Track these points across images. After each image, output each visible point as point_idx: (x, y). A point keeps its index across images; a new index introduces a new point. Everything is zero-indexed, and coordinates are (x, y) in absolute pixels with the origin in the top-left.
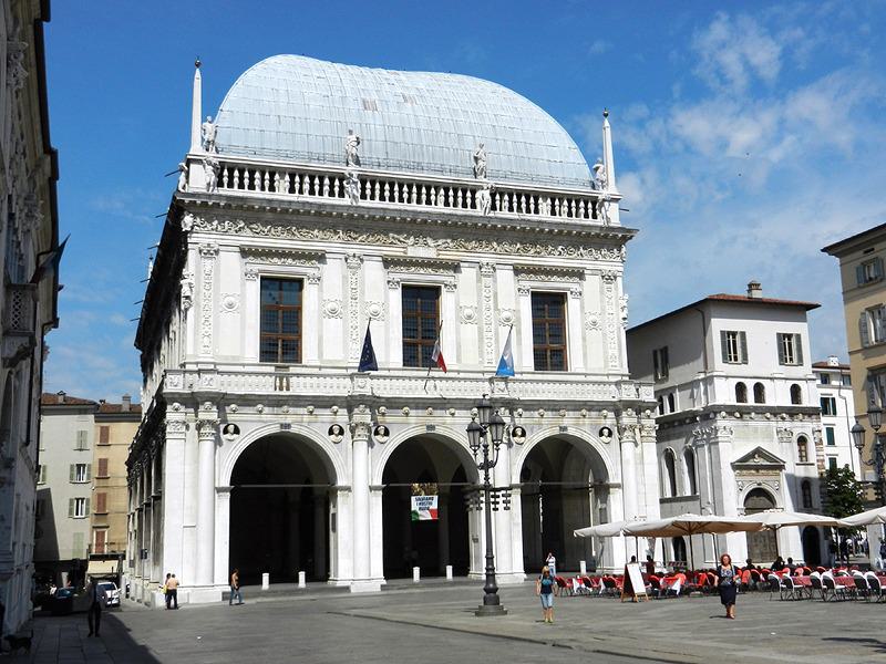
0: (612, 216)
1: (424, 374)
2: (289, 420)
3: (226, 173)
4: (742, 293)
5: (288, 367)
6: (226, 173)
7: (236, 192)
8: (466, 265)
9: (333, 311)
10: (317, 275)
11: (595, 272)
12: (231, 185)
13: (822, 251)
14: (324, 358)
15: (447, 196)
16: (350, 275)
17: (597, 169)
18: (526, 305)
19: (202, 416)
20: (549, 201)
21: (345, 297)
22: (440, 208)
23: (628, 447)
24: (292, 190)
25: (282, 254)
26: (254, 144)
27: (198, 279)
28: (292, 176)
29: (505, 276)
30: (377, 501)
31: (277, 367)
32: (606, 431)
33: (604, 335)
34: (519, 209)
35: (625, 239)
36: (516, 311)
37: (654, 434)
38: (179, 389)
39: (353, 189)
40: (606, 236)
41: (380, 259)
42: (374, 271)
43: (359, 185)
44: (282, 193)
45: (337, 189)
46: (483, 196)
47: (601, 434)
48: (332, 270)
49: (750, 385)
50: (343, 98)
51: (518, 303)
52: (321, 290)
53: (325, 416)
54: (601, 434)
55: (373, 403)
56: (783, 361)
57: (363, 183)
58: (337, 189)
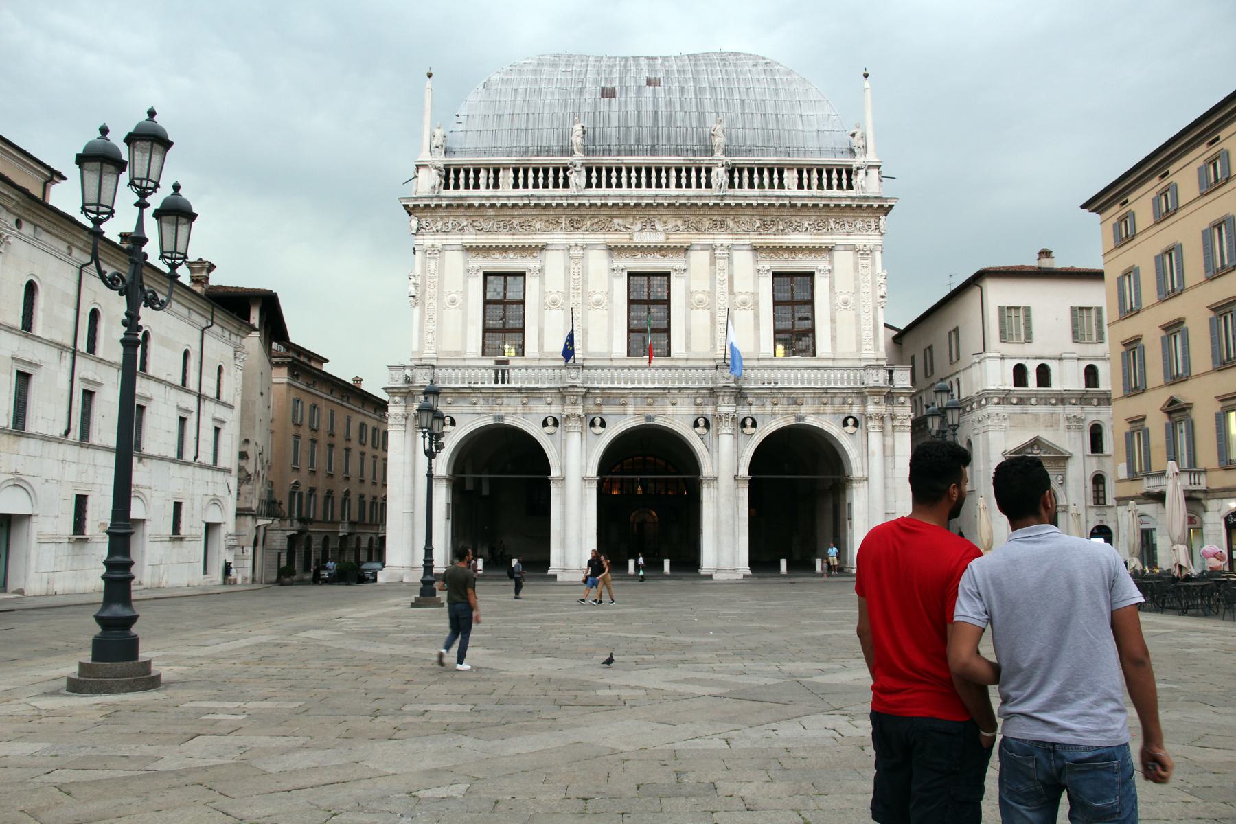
0: (868, 185)
2: (503, 412)
3: (452, 175)
4: (1031, 261)
6: (452, 175)
8: (699, 247)
9: (554, 302)
10: (539, 267)
11: (847, 248)
12: (457, 186)
13: (1084, 206)
14: (546, 349)
15: (679, 178)
16: (573, 265)
17: (853, 135)
18: (767, 284)
20: (795, 174)
21: (567, 288)
23: (875, 439)
24: (516, 186)
25: (504, 249)
26: (486, 143)
27: (424, 278)
28: (516, 171)
29: (743, 259)
31: (498, 362)
32: (850, 421)
33: (858, 316)
34: (761, 186)
35: (886, 210)
36: (755, 294)
37: (909, 424)
39: (578, 179)
40: (860, 207)
41: (604, 247)
42: (598, 261)
43: (584, 173)
45: (561, 181)
46: (719, 175)
48: (554, 261)
49: (1032, 368)
50: (581, 91)
51: (756, 284)
52: (542, 282)
53: (542, 409)
54: (845, 424)
55: (587, 393)
56: (1076, 336)
57: (589, 171)
58: (561, 181)
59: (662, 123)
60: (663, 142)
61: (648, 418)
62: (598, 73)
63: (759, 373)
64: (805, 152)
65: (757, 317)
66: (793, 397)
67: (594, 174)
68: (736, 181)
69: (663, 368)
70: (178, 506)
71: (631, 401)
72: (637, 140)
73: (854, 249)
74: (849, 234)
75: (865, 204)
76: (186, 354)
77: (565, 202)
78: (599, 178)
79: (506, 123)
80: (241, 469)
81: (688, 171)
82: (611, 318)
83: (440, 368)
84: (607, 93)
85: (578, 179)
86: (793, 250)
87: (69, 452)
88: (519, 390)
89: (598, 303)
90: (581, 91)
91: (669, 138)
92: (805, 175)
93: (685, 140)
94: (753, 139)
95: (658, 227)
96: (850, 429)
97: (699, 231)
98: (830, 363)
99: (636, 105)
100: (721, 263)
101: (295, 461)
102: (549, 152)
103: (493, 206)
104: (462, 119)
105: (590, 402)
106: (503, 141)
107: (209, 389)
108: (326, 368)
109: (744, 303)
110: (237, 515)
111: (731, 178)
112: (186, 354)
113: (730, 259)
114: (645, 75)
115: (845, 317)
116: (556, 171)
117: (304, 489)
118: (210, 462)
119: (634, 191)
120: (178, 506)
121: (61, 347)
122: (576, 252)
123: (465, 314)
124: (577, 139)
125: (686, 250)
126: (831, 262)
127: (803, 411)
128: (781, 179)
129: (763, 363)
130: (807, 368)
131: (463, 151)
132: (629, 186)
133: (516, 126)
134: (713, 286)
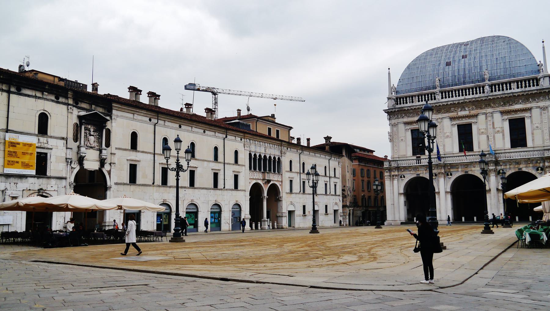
1: (464, 154)
5: (420, 157)
7: (402, 105)
11: (537, 107)
15: (473, 91)
18: (507, 125)
19: (393, 173)
20: (516, 84)
22: (471, 96)
24: (419, 101)
26: (408, 88)
28: (418, 97)
29: (497, 117)
30: (449, 197)
31: (417, 157)
34: (503, 90)
36: (502, 128)
38: (387, 166)
39: (439, 97)
43: (440, 94)
44: (416, 103)
46: (487, 88)
47: (537, 170)
51: (503, 124)
55: (445, 166)
57: (442, 93)
59: (467, 72)
60: (467, 79)
61: (466, 172)
62: (446, 56)
63: (504, 155)
64: (520, 75)
65: (503, 135)
66: (517, 162)
67: (444, 94)
68: (494, 89)
69: (470, 155)
70: (326, 206)
71: (460, 167)
72: (458, 80)
73: (539, 107)
74: (537, 102)
75: (543, 91)
76: (325, 167)
77: (434, 105)
78: (446, 95)
79: (415, 80)
80: (343, 194)
81: (476, 89)
82: (452, 141)
83: (399, 160)
84: (448, 64)
85: (439, 97)
86: (516, 111)
87: (301, 196)
88: (424, 166)
89: (448, 136)
90: (439, 65)
91: (469, 77)
92: (519, 83)
93: (475, 77)
94: (500, 73)
95: (466, 109)
96: (540, 172)
97: (481, 108)
98: (532, 149)
99: (460, 66)
100: (489, 119)
101: (363, 188)
102: (429, 89)
103: (412, 109)
104: (401, 80)
105: (446, 168)
106: (414, 87)
107: (332, 174)
108: (374, 154)
109: (498, 131)
110: (343, 207)
111: (492, 89)
112: (325, 167)
113: (492, 116)
114: (462, 54)
115: (537, 133)
116: (431, 95)
117: (366, 197)
118: (334, 194)
119: (458, 98)
120: (326, 206)
121: (297, 173)
122: (439, 120)
123: (406, 143)
124: (437, 83)
125: (476, 116)
126: (531, 113)
127: (521, 166)
128: (510, 86)
129: (506, 151)
130: (521, 152)
131: (402, 92)
132: (456, 96)
133: (418, 80)
134: (487, 127)
